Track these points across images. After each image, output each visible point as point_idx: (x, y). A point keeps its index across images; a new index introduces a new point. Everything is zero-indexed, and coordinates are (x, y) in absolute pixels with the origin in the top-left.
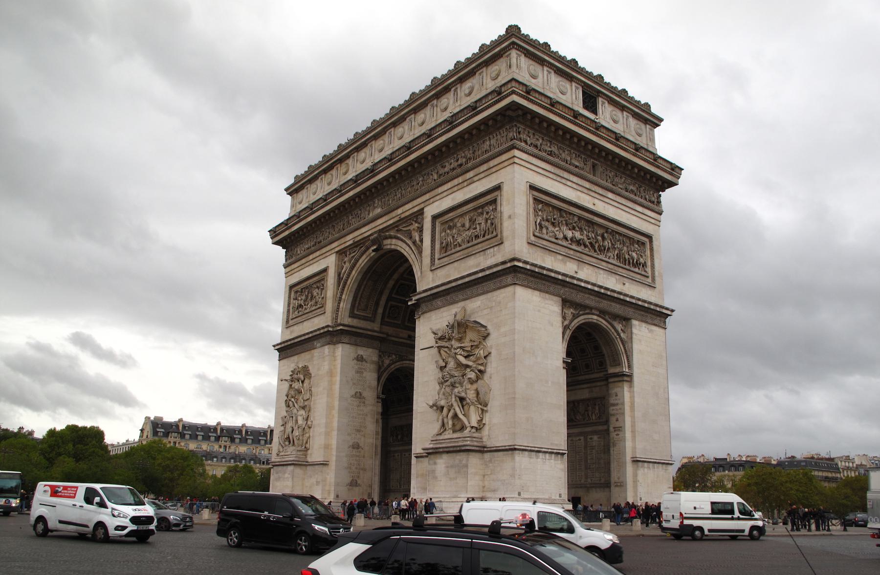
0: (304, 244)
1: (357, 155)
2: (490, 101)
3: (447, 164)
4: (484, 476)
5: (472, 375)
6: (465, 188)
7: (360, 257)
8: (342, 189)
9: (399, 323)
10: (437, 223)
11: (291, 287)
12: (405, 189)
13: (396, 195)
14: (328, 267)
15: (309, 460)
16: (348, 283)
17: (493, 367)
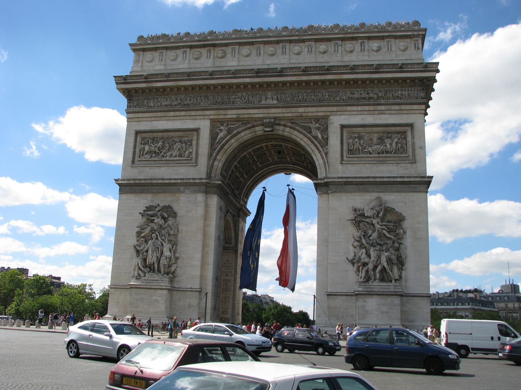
0: (160, 100)
1: (239, 49)
2: (415, 68)
3: (356, 93)
4: (402, 312)
5: (396, 245)
6: (375, 115)
7: (243, 131)
8: (236, 73)
9: (229, 183)
10: (344, 131)
11: (137, 133)
12: (307, 96)
13: (296, 97)
14: (200, 128)
15: (176, 286)
16: (226, 147)
17: (408, 241)
